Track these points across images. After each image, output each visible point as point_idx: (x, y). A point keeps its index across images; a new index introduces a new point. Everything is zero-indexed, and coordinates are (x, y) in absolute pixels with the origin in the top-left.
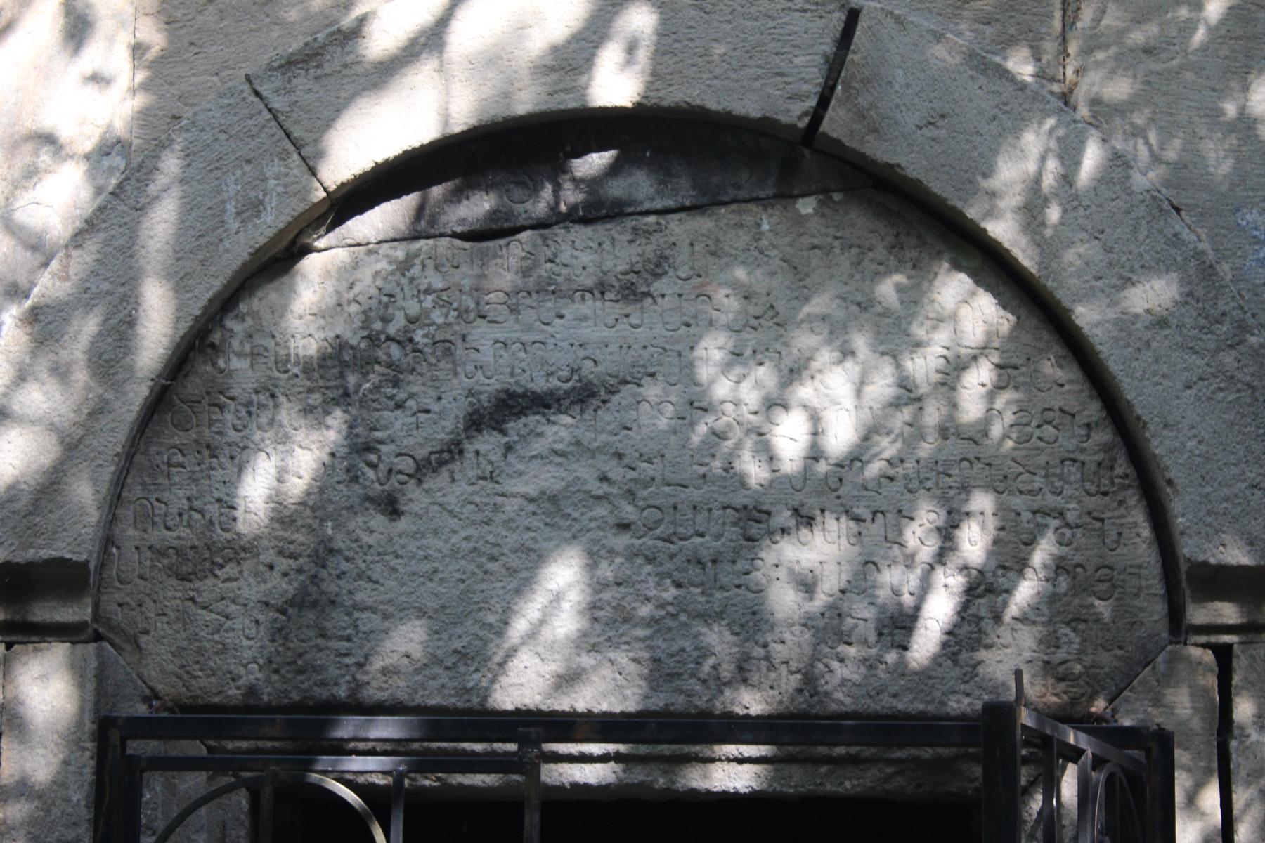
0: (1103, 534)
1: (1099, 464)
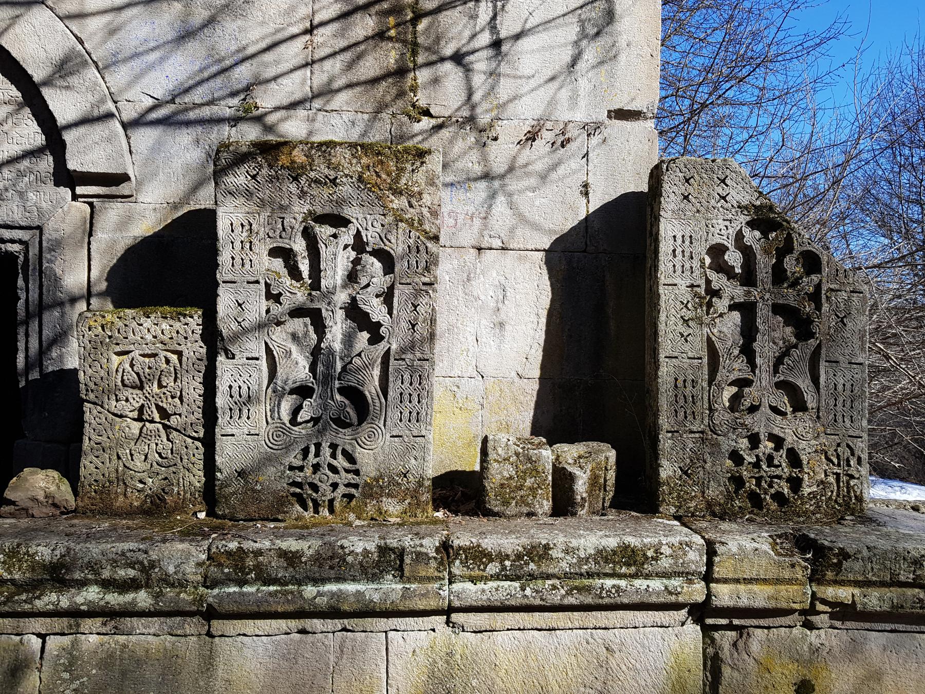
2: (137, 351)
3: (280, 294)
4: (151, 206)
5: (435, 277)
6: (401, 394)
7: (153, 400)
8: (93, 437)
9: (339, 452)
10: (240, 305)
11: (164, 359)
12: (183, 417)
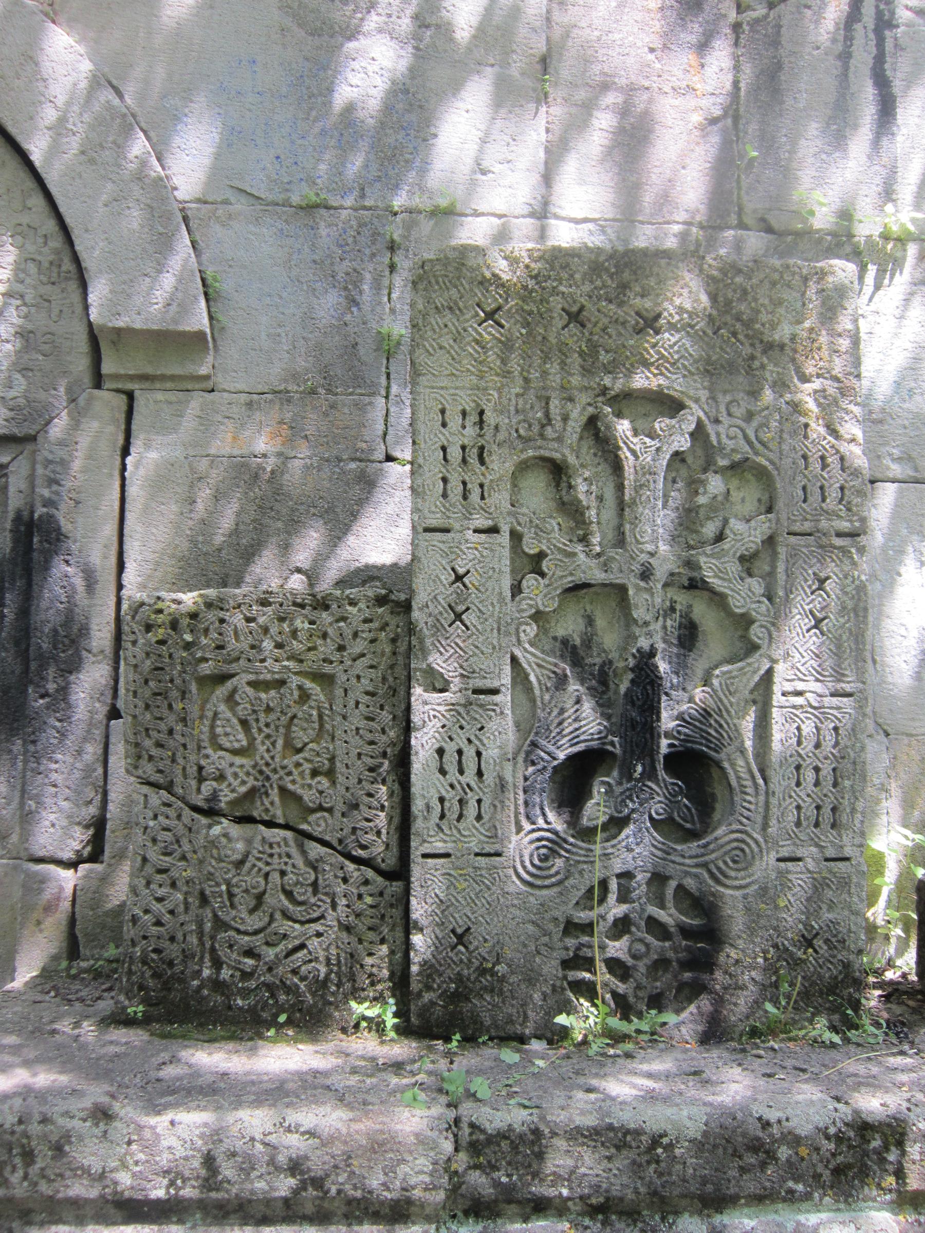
0: (50, 311)
1: (51, 263)
2: (243, 675)
3: (541, 555)
4: (243, 398)
5: (863, 520)
6: (798, 768)
7: (274, 777)
8: (153, 854)
9: (670, 891)
10: (459, 578)
11: (296, 694)
12: (338, 814)
